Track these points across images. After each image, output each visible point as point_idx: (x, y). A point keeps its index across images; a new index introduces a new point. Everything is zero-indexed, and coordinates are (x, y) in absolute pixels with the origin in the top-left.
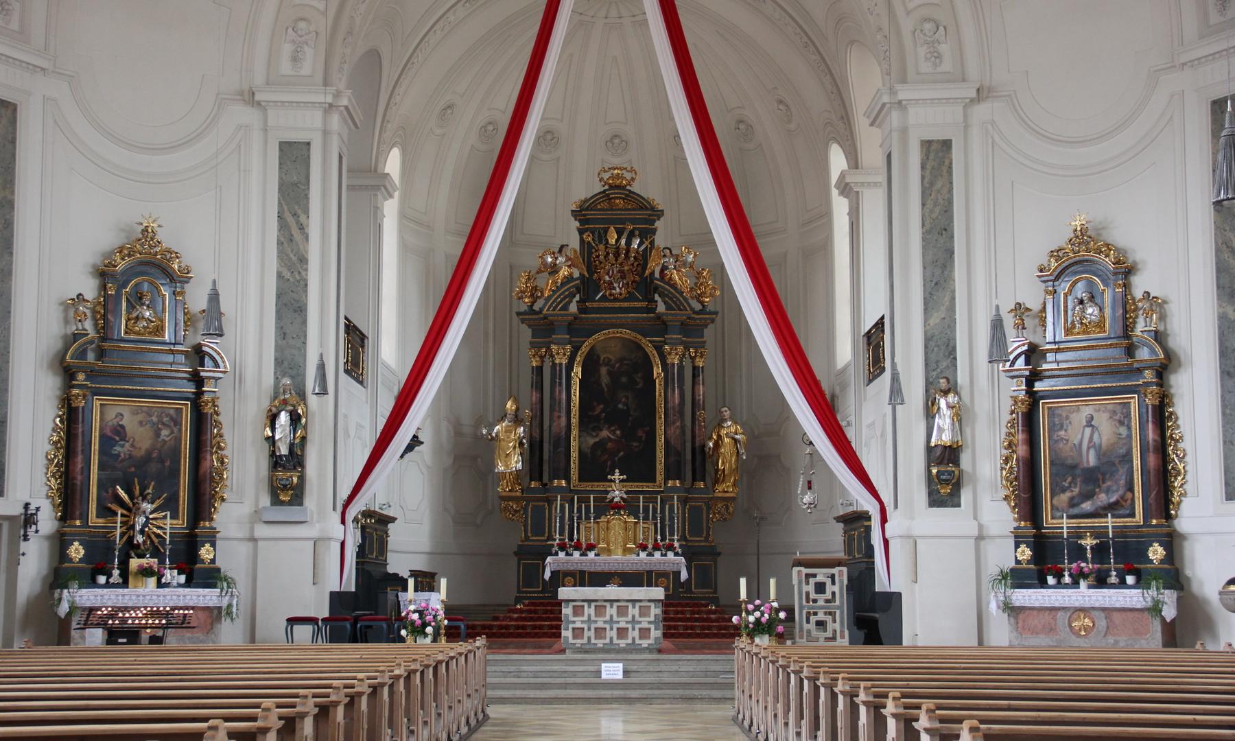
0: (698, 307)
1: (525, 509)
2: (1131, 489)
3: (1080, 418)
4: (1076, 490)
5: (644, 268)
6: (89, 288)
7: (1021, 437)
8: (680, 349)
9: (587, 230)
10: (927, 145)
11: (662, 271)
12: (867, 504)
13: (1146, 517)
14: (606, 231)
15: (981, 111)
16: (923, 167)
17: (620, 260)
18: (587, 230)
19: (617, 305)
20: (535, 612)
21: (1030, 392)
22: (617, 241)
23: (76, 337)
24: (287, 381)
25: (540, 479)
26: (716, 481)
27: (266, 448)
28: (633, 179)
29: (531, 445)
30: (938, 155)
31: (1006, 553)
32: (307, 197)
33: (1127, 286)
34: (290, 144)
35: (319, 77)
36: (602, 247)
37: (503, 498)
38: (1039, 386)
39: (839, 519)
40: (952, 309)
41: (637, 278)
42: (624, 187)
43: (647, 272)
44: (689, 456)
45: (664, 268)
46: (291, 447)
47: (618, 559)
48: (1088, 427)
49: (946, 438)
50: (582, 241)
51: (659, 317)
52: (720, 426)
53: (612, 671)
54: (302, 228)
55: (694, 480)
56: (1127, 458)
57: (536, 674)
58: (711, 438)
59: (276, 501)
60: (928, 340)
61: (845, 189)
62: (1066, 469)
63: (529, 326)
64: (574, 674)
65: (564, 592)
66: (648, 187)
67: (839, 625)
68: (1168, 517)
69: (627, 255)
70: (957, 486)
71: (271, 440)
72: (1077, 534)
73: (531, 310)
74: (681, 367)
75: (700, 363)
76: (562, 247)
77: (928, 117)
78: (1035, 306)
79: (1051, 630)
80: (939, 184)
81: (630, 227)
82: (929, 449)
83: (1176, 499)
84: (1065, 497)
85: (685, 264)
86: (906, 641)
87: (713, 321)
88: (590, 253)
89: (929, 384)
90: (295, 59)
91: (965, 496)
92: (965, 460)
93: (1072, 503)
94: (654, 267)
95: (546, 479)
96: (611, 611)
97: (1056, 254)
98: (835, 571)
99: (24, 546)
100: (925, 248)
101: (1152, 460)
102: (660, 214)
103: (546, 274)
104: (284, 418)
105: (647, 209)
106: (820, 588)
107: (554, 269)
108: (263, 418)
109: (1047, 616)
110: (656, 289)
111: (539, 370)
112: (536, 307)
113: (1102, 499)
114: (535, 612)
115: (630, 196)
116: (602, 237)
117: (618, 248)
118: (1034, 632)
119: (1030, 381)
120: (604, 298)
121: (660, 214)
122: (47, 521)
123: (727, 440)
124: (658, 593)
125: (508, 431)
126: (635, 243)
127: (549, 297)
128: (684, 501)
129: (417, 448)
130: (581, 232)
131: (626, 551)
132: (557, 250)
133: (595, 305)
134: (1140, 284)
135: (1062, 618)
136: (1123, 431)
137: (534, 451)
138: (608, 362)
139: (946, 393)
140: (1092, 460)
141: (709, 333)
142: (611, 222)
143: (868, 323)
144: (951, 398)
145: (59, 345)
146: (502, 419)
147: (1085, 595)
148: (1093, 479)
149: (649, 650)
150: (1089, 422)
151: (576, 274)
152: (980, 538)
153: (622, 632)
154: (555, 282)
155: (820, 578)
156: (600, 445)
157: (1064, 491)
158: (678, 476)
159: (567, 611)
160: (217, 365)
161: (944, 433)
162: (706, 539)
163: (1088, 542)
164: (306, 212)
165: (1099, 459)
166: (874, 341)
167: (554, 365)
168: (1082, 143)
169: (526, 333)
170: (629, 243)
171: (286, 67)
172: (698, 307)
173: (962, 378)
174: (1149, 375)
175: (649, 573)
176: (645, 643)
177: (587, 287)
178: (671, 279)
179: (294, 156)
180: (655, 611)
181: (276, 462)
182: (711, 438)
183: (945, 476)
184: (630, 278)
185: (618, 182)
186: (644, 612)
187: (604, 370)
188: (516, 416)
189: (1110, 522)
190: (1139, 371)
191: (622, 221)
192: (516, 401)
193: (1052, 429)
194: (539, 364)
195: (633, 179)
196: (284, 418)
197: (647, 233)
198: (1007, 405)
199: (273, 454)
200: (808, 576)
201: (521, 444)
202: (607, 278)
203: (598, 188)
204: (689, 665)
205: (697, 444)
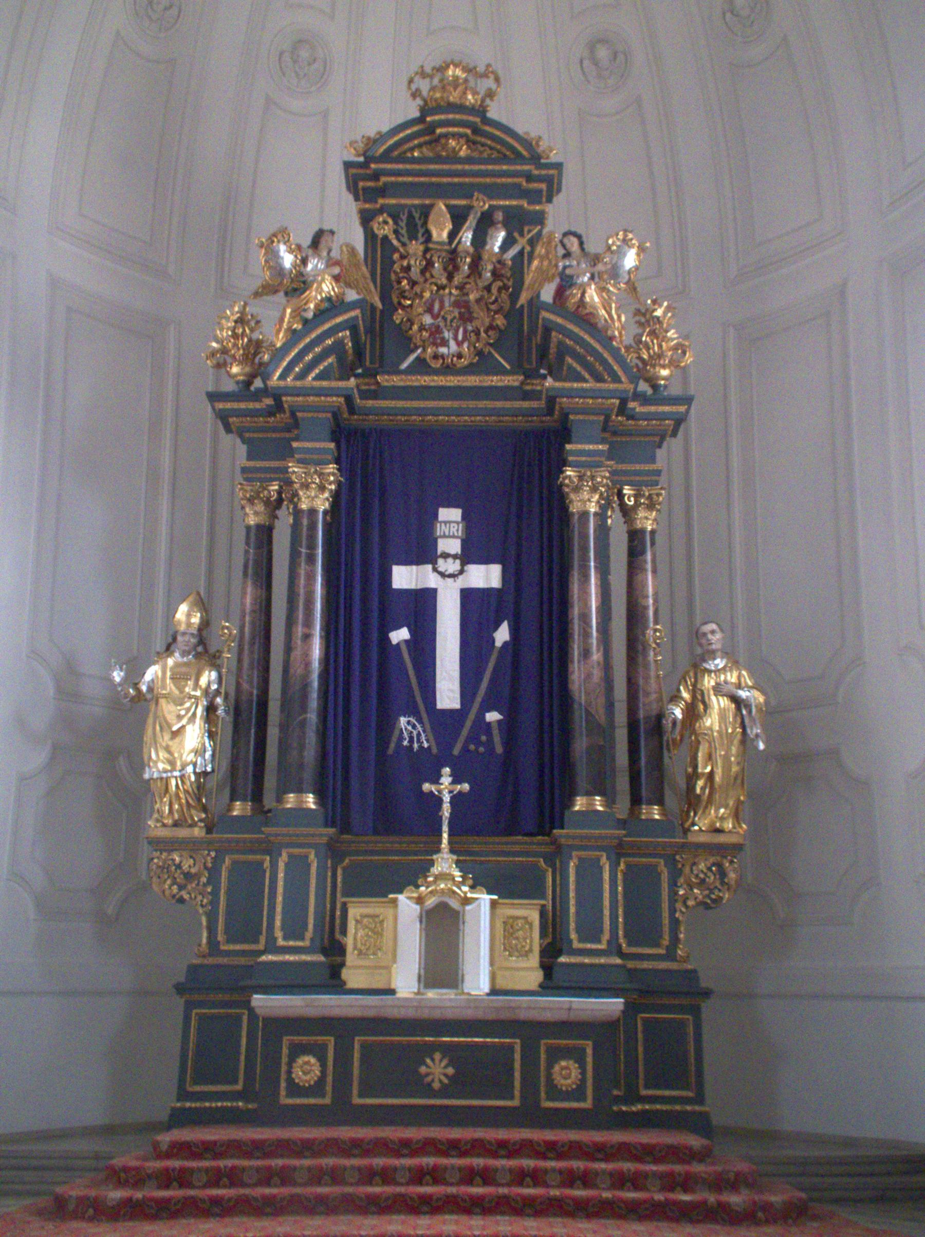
0: (643, 387)
1: (214, 873)
5: (514, 297)
8: (602, 476)
9: (381, 210)
11: (560, 293)
14: (426, 212)
17: (457, 280)
18: (381, 210)
19: (452, 381)
20: (182, 1179)
22: (453, 235)
25: (257, 796)
26: (692, 802)
28: (490, 94)
29: (237, 711)
36: (416, 247)
37: (159, 844)
41: (500, 321)
42: (472, 110)
43: (523, 299)
44: (621, 735)
45: (566, 283)
50: (370, 237)
52: (697, 667)
55: (636, 800)
58: (675, 698)
63: (240, 434)
66: (524, 109)
74: (603, 530)
75: (647, 521)
81: (482, 204)
85: (614, 272)
87: (679, 421)
88: (388, 264)
95: (269, 801)
103: (280, 297)
105: (518, 155)
107: (298, 285)
111: (263, 536)
112: (258, 383)
114: (182, 1179)
116: (416, 225)
117: (454, 252)
123: (718, 704)
125: (179, 678)
127: (286, 348)
130: (366, 219)
132: (306, 242)
133: (396, 381)
137: (245, 722)
141: (668, 456)
142: (441, 191)
146: (168, 649)
151: (352, 296)
154: (298, 312)
162: (670, 955)
167: (297, 513)
169: (235, 451)
170: (480, 240)
172: (643, 387)
178: (582, 303)
182: (675, 698)
185: (454, 97)
188: (202, 641)
191: (466, 192)
192: (202, 604)
194: (262, 519)
195: (490, 94)
201: (211, 709)
202: (428, 320)
205: (641, 714)
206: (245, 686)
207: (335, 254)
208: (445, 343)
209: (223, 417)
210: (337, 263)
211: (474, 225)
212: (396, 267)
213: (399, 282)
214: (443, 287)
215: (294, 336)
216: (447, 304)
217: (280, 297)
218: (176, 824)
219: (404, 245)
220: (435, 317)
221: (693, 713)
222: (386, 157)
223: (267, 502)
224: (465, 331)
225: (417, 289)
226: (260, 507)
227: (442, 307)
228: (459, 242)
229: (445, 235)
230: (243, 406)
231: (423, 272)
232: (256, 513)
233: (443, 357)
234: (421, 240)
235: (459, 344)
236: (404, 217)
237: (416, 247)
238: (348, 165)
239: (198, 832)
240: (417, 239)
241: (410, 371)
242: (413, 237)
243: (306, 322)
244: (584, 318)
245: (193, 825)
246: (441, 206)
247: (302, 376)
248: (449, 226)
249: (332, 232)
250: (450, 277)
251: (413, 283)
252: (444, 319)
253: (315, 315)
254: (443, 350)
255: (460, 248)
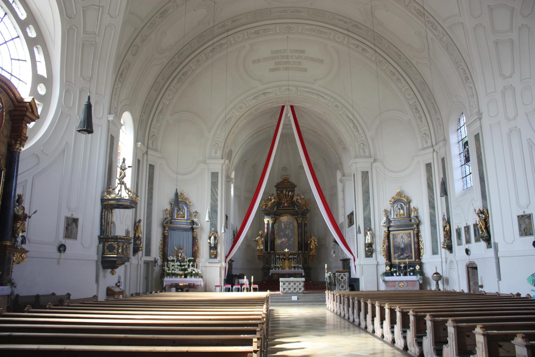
2: (411, 252)
3: (400, 236)
4: (399, 253)
6: (168, 207)
7: (387, 241)
10: (363, 172)
12: (349, 255)
13: (415, 259)
15: (375, 164)
16: (362, 177)
21: (388, 230)
23: (166, 219)
24: (213, 229)
26: (311, 251)
27: (208, 245)
30: (365, 175)
31: (384, 268)
32: (218, 185)
33: (409, 205)
34: (214, 173)
35: (221, 157)
38: (390, 229)
39: (341, 260)
40: (370, 211)
45: (297, 199)
46: (214, 245)
47: (287, 270)
48: (402, 238)
49: (369, 241)
51: (296, 211)
52: (311, 237)
53: (294, 298)
54: (217, 192)
56: (411, 246)
57: (276, 299)
59: (211, 257)
60: (365, 218)
61: (341, 181)
62: (397, 248)
64: (285, 299)
65: (281, 279)
67: (346, 286)
68: (420, 259)
70: (372, 253)
71: (210, 243)
72: (400, 263)
73: (266, 210)
74: (301, 223)
75: (306, 222)
77: (362, 165)
78: (389, 210)
79: (394, 286)
80: (366, 181)
82: (365, 244)
83: (421, 254)
84: (396, 255)
86: (360, 290)
89: (365, 228)
90: (216, 153)
91: (374, 255)
92: (374, 246)
93: (399, 256)
94: (295, 199)
96: (292, 284)
97: (393, 198)
98: (346, 274)
99: (155, 268)
100: (363, 196)
101: (416, 246)
102: (295, 186)
104: (212, 238)
106: (342, 278)
107: (271, 200)
108: (207, 237)
109: (393, 283)
110: (295, 204)
113: (405, 255)
115: (289, 182)
116: (282, 192)
118: (391, 287)
119: (388, 228)
121: (295, 186)
122: (160, 262)
124: (303, 279)
126: (290, 193)
128: (303, 256)
130: (277, 191)
131: (290, 268)
134: (412, 205)
135: (397, 283)
136: (410, 239)
137: (266, 244)
138: (284, 222)
139: (369, 230)
140: (403, 246)
141: (308, 215)
142: (284, 188)
143: (348, 213)
144: (371, 232)
145: (162, 221)
147: (402, 278)
148: (403, 250)
149: (301, 293)
150: (402, 237)
152: (377, 265)
153: (295, 289)
155: (342, 275)
156: (283, 242)
157: (396, 253)
158: (302, 250)
159: (281, 284)
160: (197, 225)
161: (369, 239)
163: (402, 265)
164: (217, 188)
165: (404, 245)
166: (351, 218)
168: (398, 172)
170: (288, 193)
171: (213, 155)
173: (372, 227)
174: (415, 226)
175: (295, 274)
176: (300, 291)
177: (278, 204)
179: (214, 175)
180: (302, 284)
181: (211, 248)
183: (370, 250)
184: (289, 202)
186: (300, 284)
187: (283, 224)
189: (407, 261)
190: (412, 225)
191: (287, 188)
193: (393, 239)
196: (212, 238)
197: (293, 191)
198: (383, 233)
199: (210, 246)
200: (340, 275)
203: (280, 180)
204: (312, 296)
221: (311, 242)
244: (299, 203)
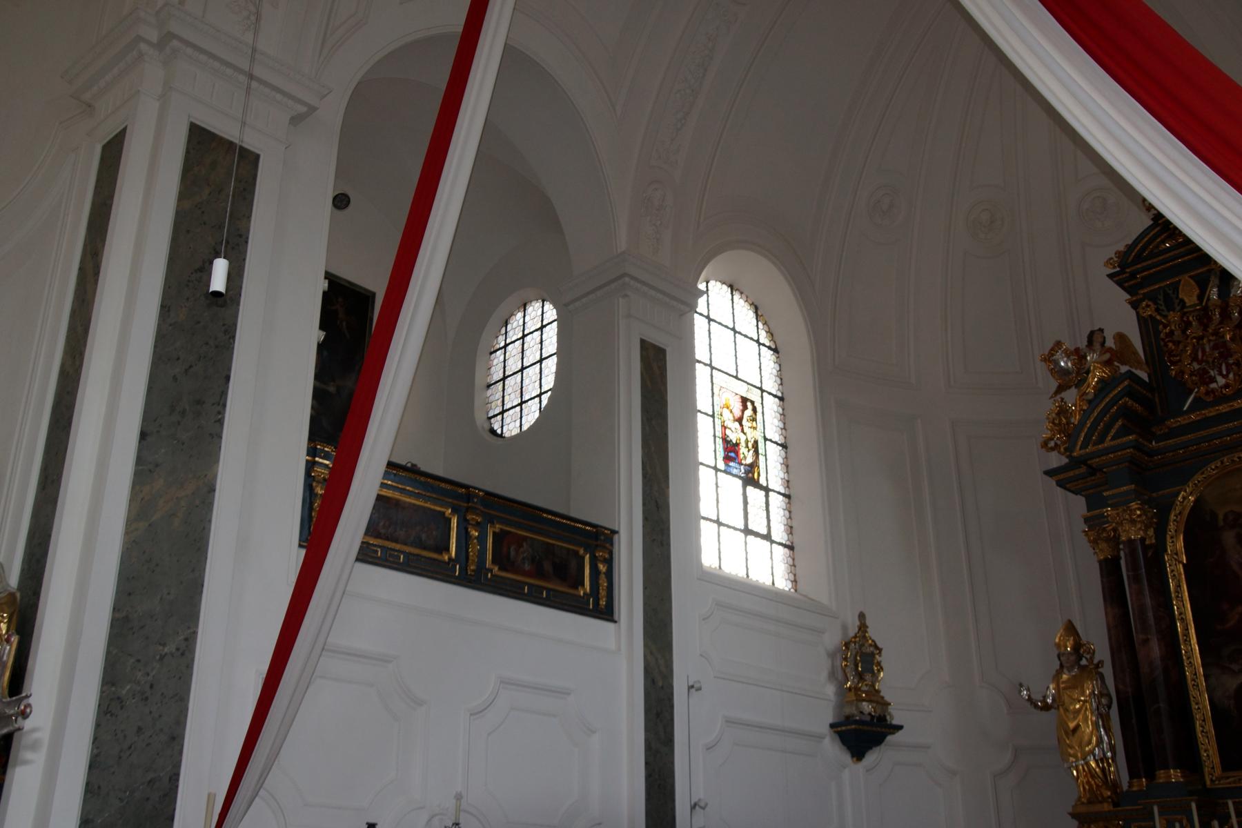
19: (1224, 408)
22: (1200, 297)
36: (1174, 317)
69: (1225, 315)
73: (1074, 463)
76: (1092, 334)
116: (1170, 300)
117: (1205, 309)
120: (1199, 404)
127: (1082, 423)
129: (889, 738)
130: (1135, 305)
132: (1082, 343)
133: (1182, 420)
202: (1196, 366)
206: (1121, 687)
207: (1110, 343)
208: (1213, 380)
209: (1060, 484)
210: (1110, 350)
211: (1217, 282)
212: (1162, 336)
213: (1166, 345)
214: (1201, 338)
215: (1085, 414)
216: (1207, 350)
217: (1073, 391)
218: (1090, 802)
219: (1165, 317)
220: (1200, 363)
222: (1139, 258)
223: (1108, 540)
224: (1228, 366)
225: (1181, 347)
226: (1103, 545)
227: (1204, 351)
228: (1208, 299)
229: (1194, 299)
230: (1071, 474)
231: (1184, 332)
232: (1101, 550)
233: (1213, 391)
234: (1178, 308)
235: (1224, 376)
236: (1161, 297)
237: (1174, 317)
238: (1111, 276)
239: (1106, 807)
240: (1174, 310)
241: (1192, 409)
242: (1170, 308)
243: (1090, 402)
245: (1104, 800)
246: (1185, 278)
247: (1101, 439)
248: (1197, 291)
249: (1101, 330)
250: (1205, 329)
251: (1177, 343)
252: (1207, 362)
253: (1095, 395)
254: (1213, 385)
255: (1210, 304)
